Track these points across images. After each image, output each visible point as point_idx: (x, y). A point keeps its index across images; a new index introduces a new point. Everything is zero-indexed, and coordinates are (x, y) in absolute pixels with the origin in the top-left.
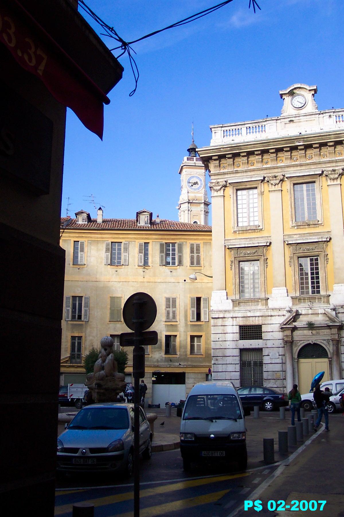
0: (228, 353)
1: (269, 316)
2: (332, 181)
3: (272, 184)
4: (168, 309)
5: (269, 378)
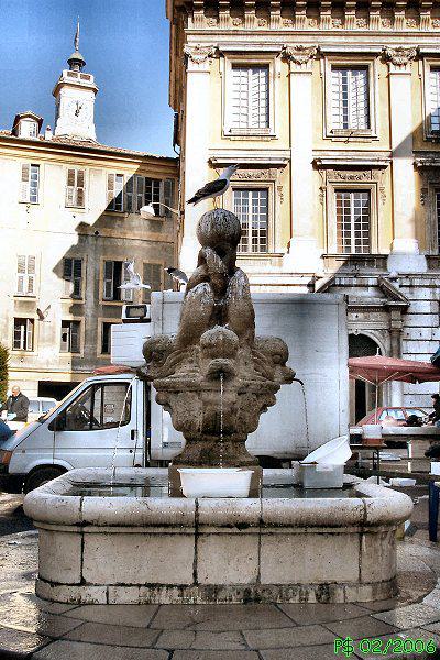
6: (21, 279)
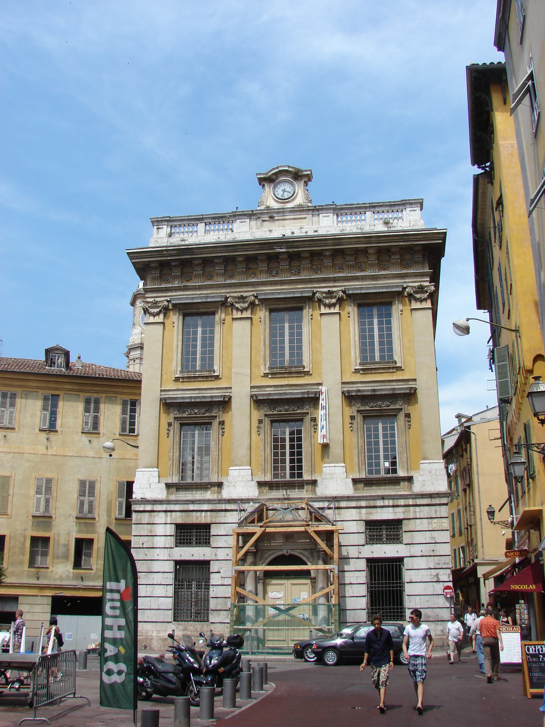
0: (156, 566)
1: (222, 511)
2: (327, 309)
3: (237, 309)
4: (82, 498)
5: (219, 607)
6: (39, 500)
